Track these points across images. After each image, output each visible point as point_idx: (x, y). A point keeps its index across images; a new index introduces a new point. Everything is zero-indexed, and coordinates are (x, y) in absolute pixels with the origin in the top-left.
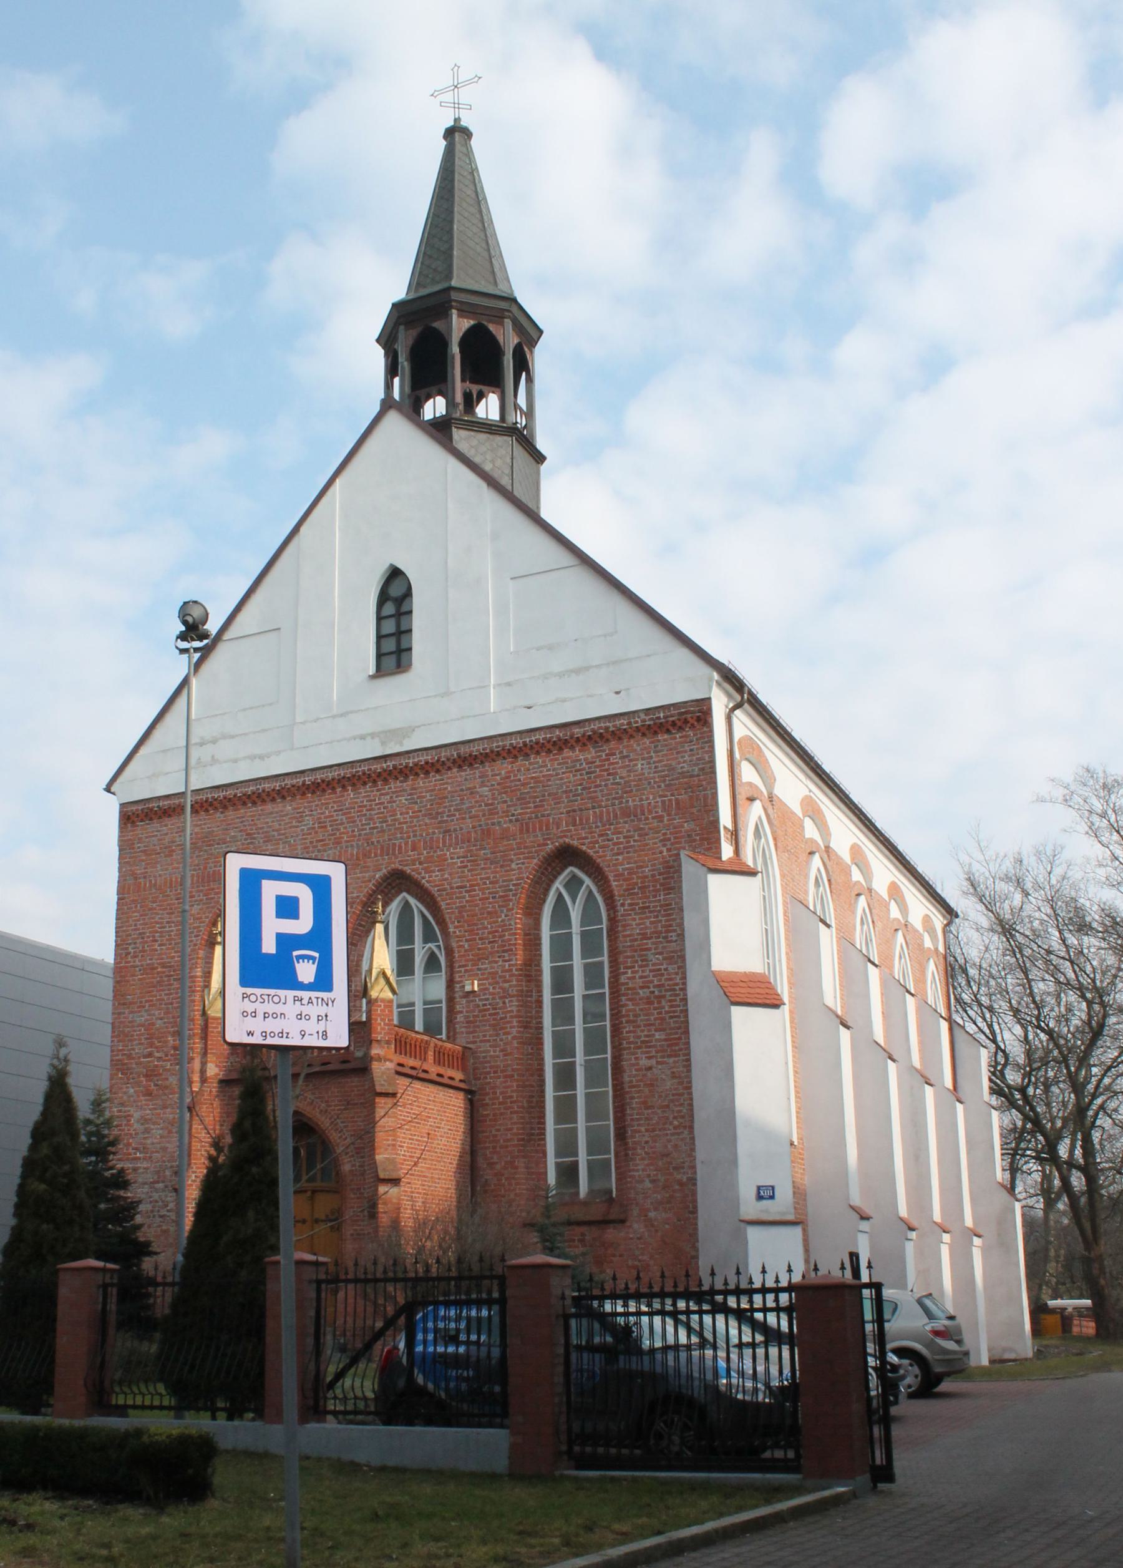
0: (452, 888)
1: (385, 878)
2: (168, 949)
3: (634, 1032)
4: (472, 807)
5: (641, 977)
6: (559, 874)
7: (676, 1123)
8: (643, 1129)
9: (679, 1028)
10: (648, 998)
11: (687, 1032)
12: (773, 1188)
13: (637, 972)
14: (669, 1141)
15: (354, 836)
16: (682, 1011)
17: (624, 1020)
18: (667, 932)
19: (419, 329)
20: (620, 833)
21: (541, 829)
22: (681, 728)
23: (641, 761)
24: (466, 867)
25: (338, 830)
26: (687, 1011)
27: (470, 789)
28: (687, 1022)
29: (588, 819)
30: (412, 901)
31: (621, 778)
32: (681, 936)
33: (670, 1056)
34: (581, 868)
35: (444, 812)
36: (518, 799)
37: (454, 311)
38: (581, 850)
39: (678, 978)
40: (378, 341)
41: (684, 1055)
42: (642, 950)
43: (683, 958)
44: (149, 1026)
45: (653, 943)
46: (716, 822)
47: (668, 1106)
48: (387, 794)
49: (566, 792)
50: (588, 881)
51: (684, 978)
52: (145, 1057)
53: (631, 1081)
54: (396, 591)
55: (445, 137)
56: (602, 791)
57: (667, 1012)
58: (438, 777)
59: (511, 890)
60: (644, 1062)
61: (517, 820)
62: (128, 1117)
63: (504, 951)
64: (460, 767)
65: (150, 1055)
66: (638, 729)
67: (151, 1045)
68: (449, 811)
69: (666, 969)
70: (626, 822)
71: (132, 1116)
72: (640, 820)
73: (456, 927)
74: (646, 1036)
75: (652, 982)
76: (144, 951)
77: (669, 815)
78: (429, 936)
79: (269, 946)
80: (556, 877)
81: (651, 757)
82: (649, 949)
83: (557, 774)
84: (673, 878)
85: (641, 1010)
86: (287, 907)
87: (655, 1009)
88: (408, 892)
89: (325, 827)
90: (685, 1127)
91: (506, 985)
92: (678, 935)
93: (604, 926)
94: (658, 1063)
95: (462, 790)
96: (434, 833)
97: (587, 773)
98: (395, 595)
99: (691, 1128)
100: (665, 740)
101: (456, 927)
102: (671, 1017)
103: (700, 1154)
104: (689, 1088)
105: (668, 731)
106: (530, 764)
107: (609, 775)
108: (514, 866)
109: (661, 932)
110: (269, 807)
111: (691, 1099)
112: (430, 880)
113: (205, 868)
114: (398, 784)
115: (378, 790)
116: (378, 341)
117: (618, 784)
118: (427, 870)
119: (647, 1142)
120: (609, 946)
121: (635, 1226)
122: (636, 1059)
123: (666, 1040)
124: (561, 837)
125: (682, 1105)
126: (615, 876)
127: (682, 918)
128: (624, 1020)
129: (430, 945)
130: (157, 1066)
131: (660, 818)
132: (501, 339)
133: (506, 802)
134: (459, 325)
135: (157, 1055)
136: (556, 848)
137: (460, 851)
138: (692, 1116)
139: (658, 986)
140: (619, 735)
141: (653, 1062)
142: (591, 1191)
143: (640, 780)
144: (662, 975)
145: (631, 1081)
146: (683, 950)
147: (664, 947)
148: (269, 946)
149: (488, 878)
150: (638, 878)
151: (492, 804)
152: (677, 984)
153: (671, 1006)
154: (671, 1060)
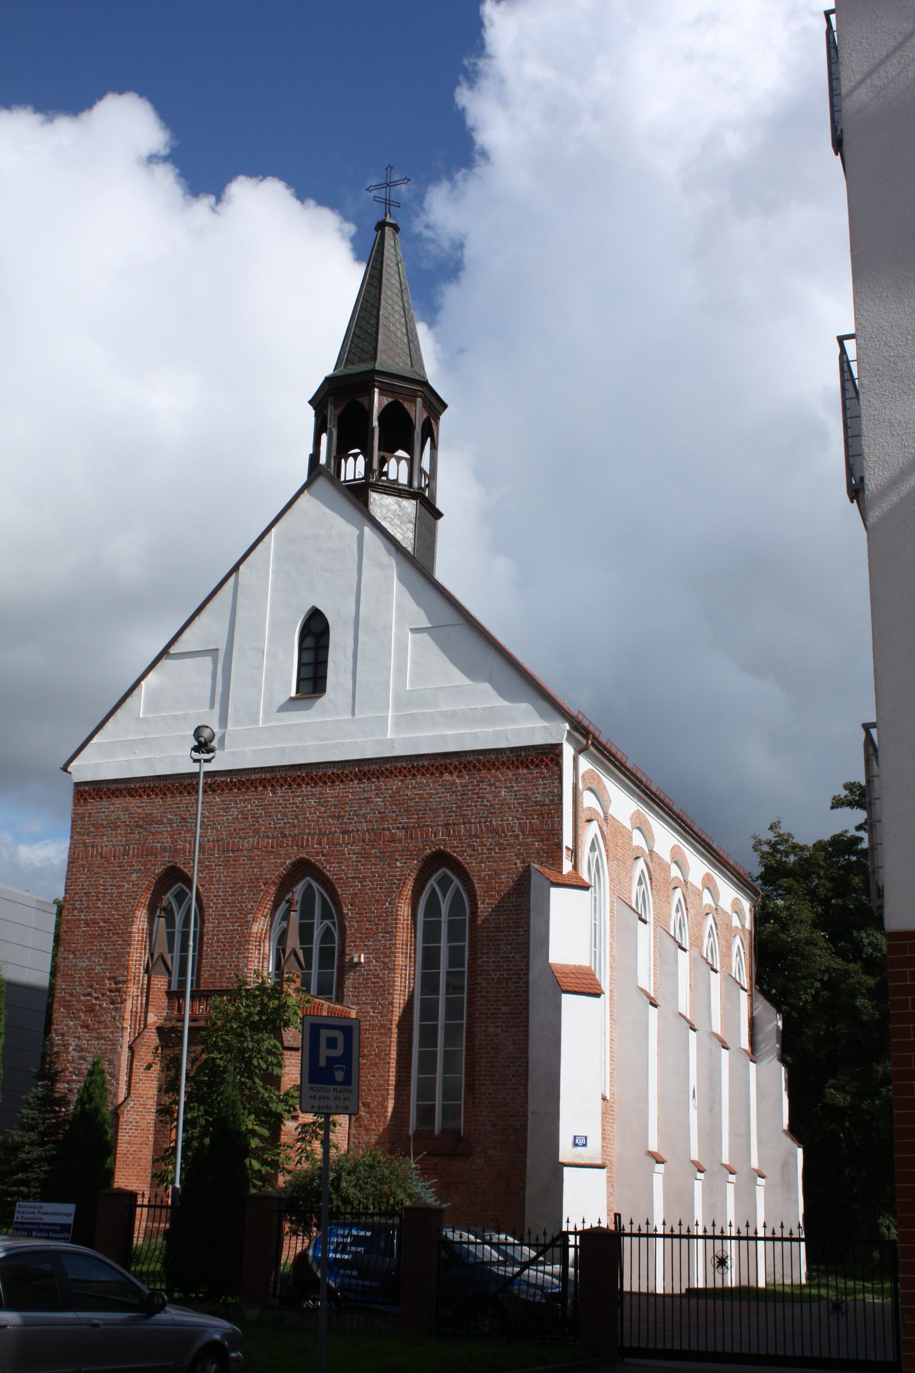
0: (347, 878)
1: (293, 864)
2: (109, 908)
3: (486, 1005)
4: (368, 813)
5: (494, 962)
6: (434, 872)
7: (514, 1080)
8: (488, 1083)
9: (521, 1005)
10: (498, 979)
11: (527, 1009)
12: (586, 1138)
13: (491, 957)
14: (509, 1094)
15: (271, 828)
16: (524, 991)
17: (478, 995)
18: (517, 927)
20: (484, 845)
21: (422, 837)
22: (537, 766)
23: (504, 788)
24: (360, 861)
25: (258, 822)
26: (528, 991)
27: (366, 798)
28: (528, 1000)
29: (460, 831)
30: (315, 885)
31: (488, 801)
32: (527, 932)
33: (512, 1027)
34: (452, 869)
35: (344, 816)
36: (405, 811)
37: (376, 390)
38: (453, 856)
39: (523, 964)
40: (310, 402)
41: (523, 1027)
42: (495, 940)
43: (528, 949)
44: (89, 970)
45: (505, 936)
46: (559, 845)
47: (509, 1066)
48: (298, 796)
49: (443, 808)
50: (456, 881)
51: (527, 965)
52: (84, 995)
53: (481, 1045)
54: (316, 627)
55: (377, 229)
56: (472, 810)
57: (512, 992)
58: (342, 786)
59: (395, 884)
60: (491, 1030)
61: (403, 828)
62: (66, 1046)
63: (386, 933)
64: (360, 779)
65: (89, 994)
66: (503, 764)
67: (91, 986)
68: (349, 815)
69: (514, 957)
70: (489, 838)
71: (70, 1045)
72: (500, 837)
73: (350, 910)
74: (495, 1009)
75: (502, 966)
76: (88, 907)
77: (524, 835)
78: (326, 914)
79: (322, 1063)
80: (431, 875)
81: (513, 787)
82: (501, 940)
83: (438, 793)
84: (523, 885)
85: (492, 988)
86: (332, 1043)
87: (503, 988)
88: (312, 877)
89: (247, 818)
90: (521, 1084)
91: (386, 960)
92: (525, 931)
93: (467, 917)
94: (503, 1031)
95: (360, 799)
96: (335, 832)
97: (461, 795)
98: (315, 632)
99: (526, 1084)
100: (524, 774)
101: (350, 910)
102: (515, 996)
103: (531, 1106)
104: (526, 1053)
105: (527, 767)
106: (416, 783)
107: (478, 797)
108: (398, 864)
109: (511, 927)
111: (527, 1062)
112: (330, 870)
113: (145, 843)
114: (309, 789)
115: (292, 792)
116: (310, 402)
117: (485, 805)
118: (328, 862)
119: (490, 1094)
120: (470, 934)
121: (477, 1160)
122: (486, 1027)
123: (510, 1014)
124: (437, 845)
125: (520, 1066)
126: (478, 879)
127: (529, 918)
128: (478, 995)
129: (326, 921)
130: (94, 1005)
131: (517, 836)
132: (413, 416)
133: (394, 812)
134: (378, 401)
135: (95, 995)
136: (433, 853)
137: (356, 848)
138: (527, 1075)
139: (507, 970)
141: (500, 1030)
142: (443, 1131)
143: (503, 804)
144: (511, 961)
145: (481, 1045)
146: (528, 943)
147: (513, 939)
148: (322, 1063)
149: (377, 872)
150: (496, 883)
151: (384, 813)
152: (522, 970)
153: (516, 987)
154: (513, 1030)
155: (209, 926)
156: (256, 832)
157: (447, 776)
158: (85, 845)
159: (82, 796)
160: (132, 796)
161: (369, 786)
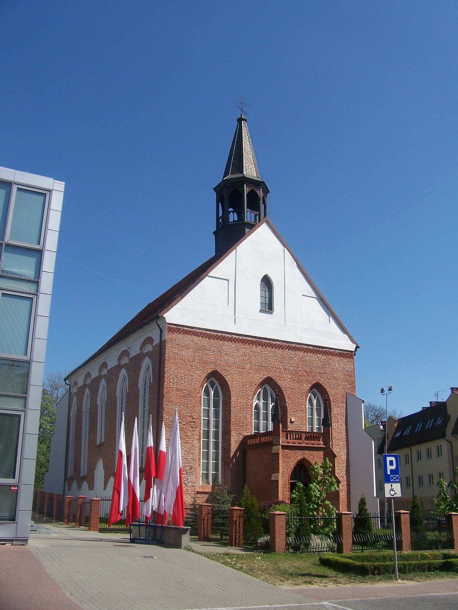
19: (250, 189)
23: (337, 363)
30: (268, 388)
110: (226, 343)
112: (281, 383)
140: (332, 354)
155: (233, 399)
156: (251, 362)
157: (318, 355)
158: (174, 353)
159: (170, 330)
160: (195, 335)
161: (292, 353)
